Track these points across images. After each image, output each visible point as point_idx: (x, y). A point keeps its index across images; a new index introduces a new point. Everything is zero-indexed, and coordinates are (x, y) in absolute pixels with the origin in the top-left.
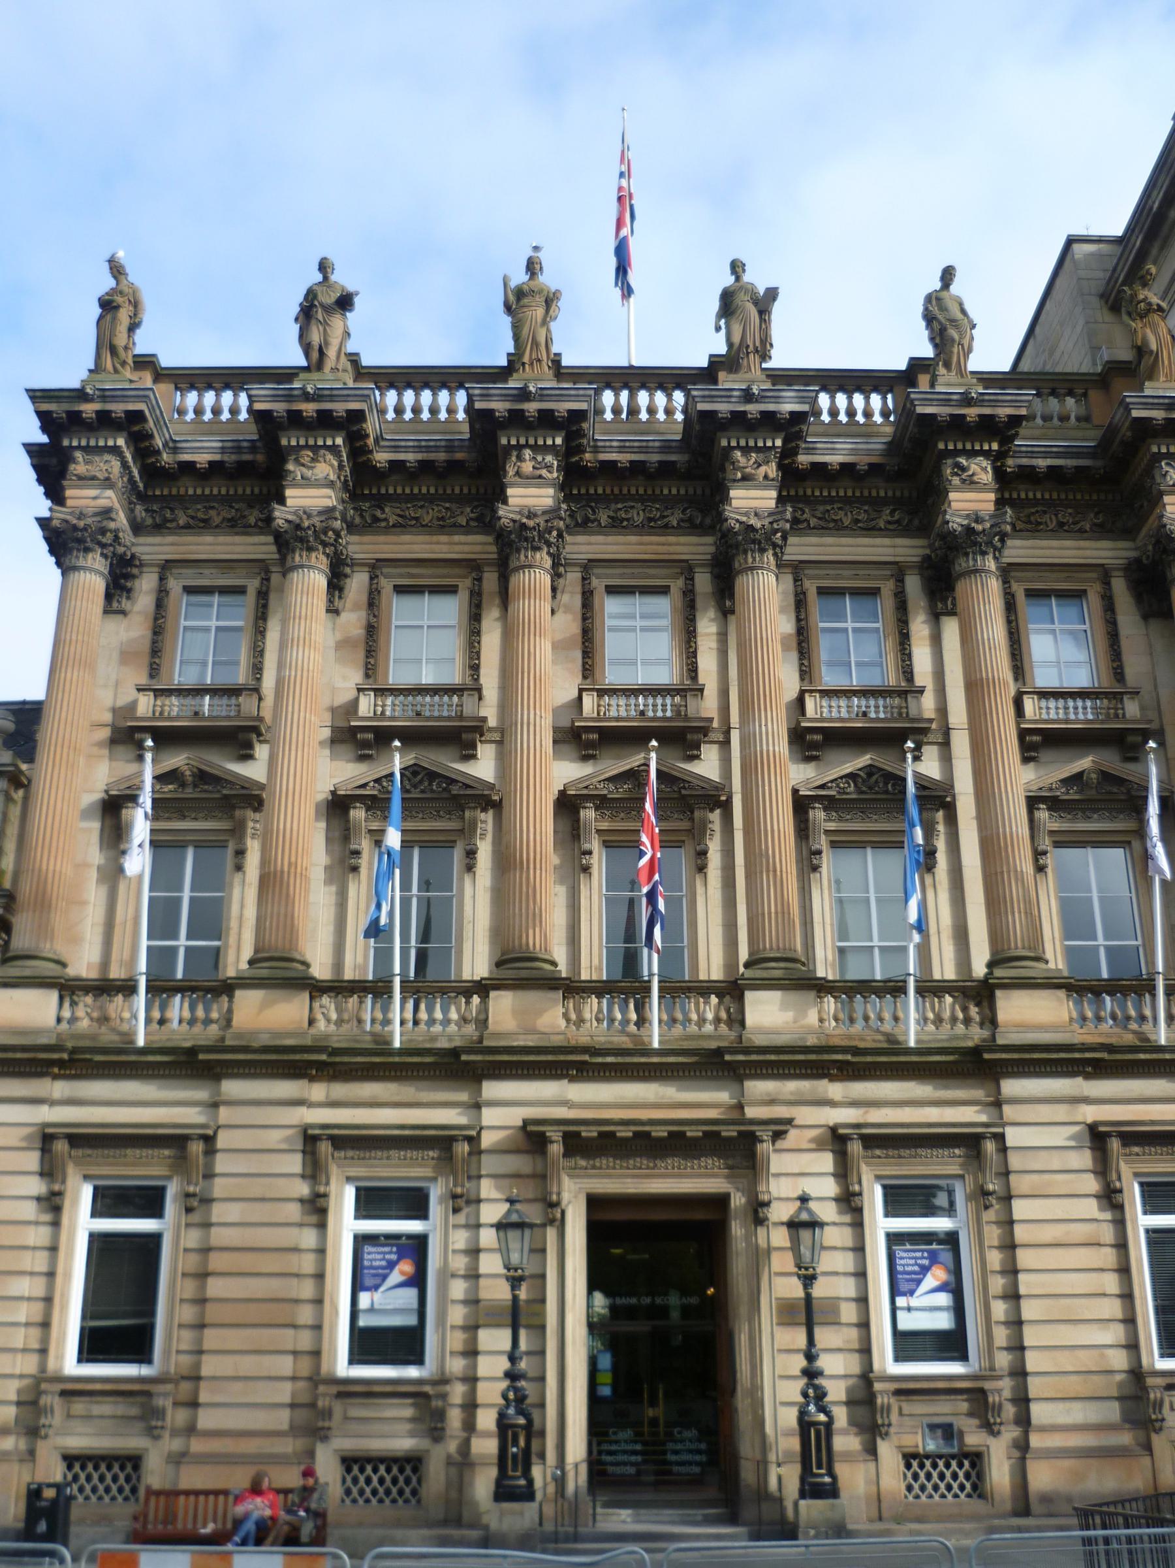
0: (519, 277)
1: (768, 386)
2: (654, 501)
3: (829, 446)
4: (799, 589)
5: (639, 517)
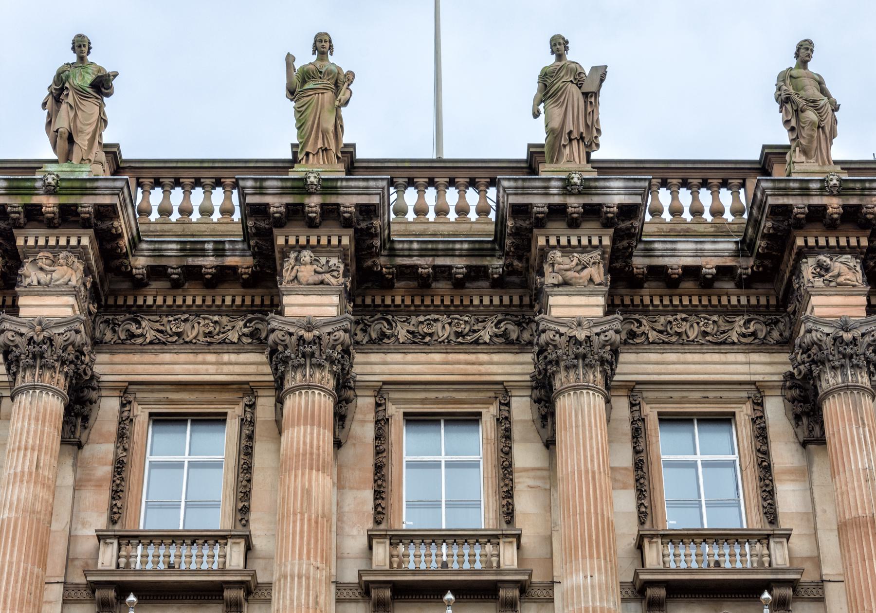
0: (305, 58)
1: (595, 175)
2: (461, 313)
3: (669, 246)
4: (637, 414)
5: (443, 330)
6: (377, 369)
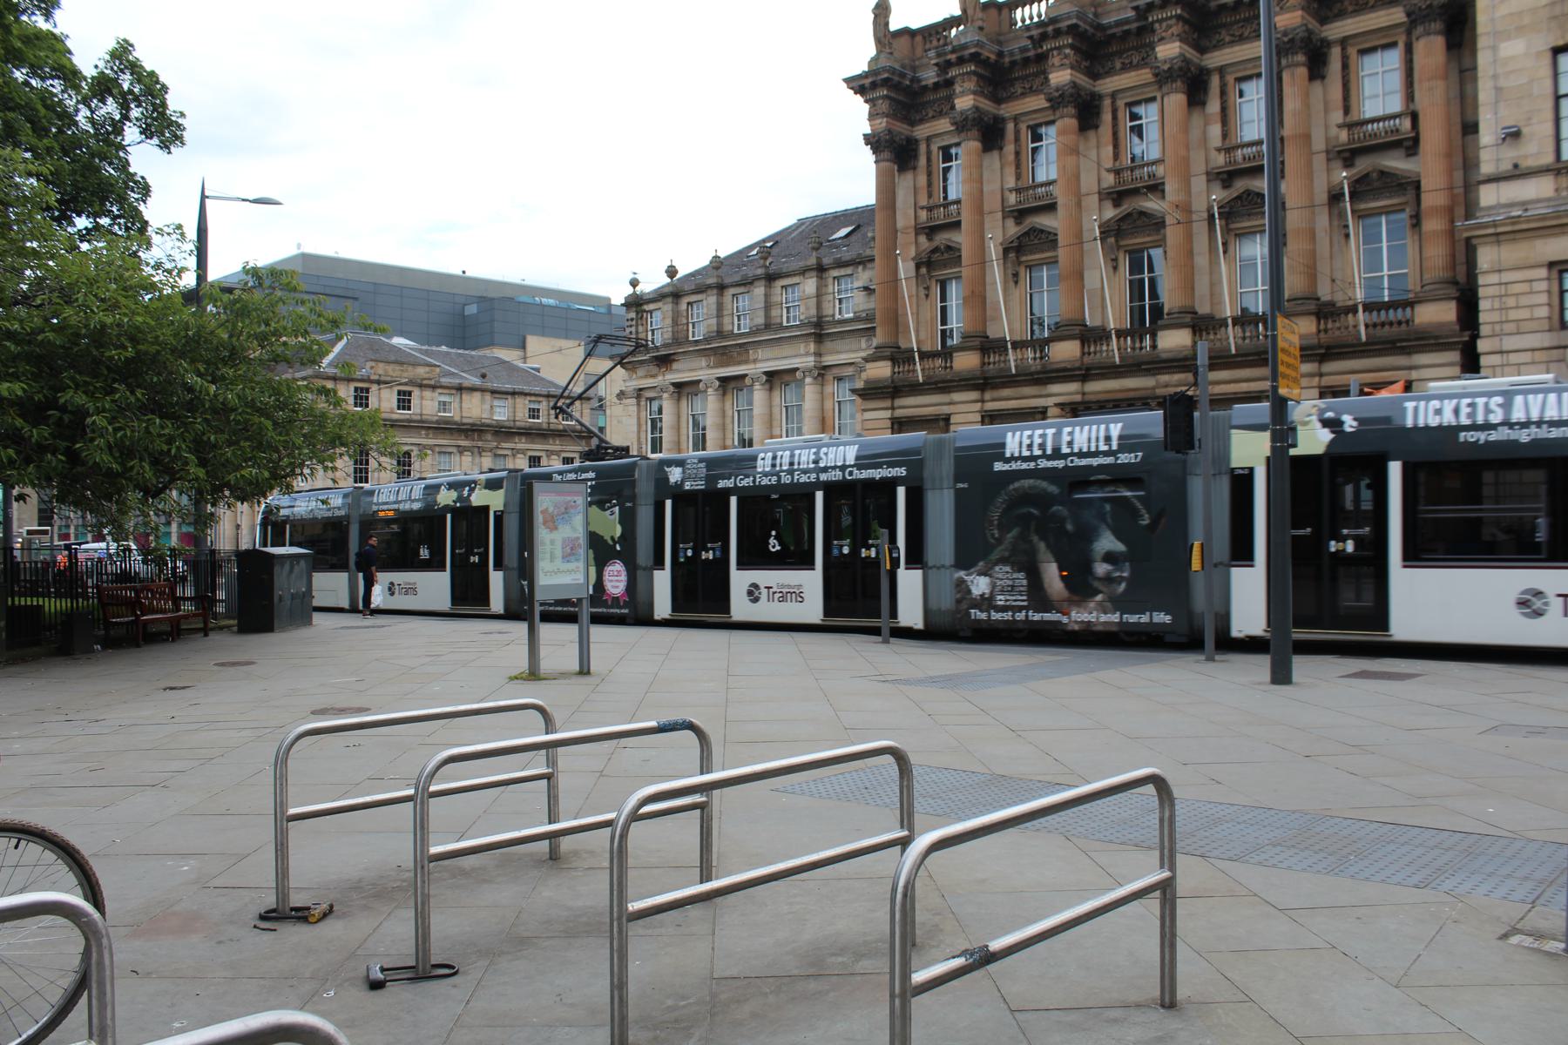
6: (1109, 86)
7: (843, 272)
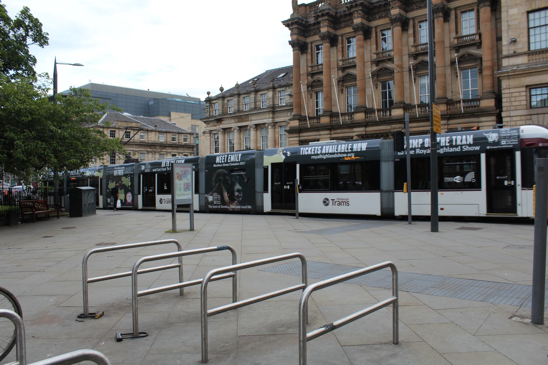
7: (282, 89)
